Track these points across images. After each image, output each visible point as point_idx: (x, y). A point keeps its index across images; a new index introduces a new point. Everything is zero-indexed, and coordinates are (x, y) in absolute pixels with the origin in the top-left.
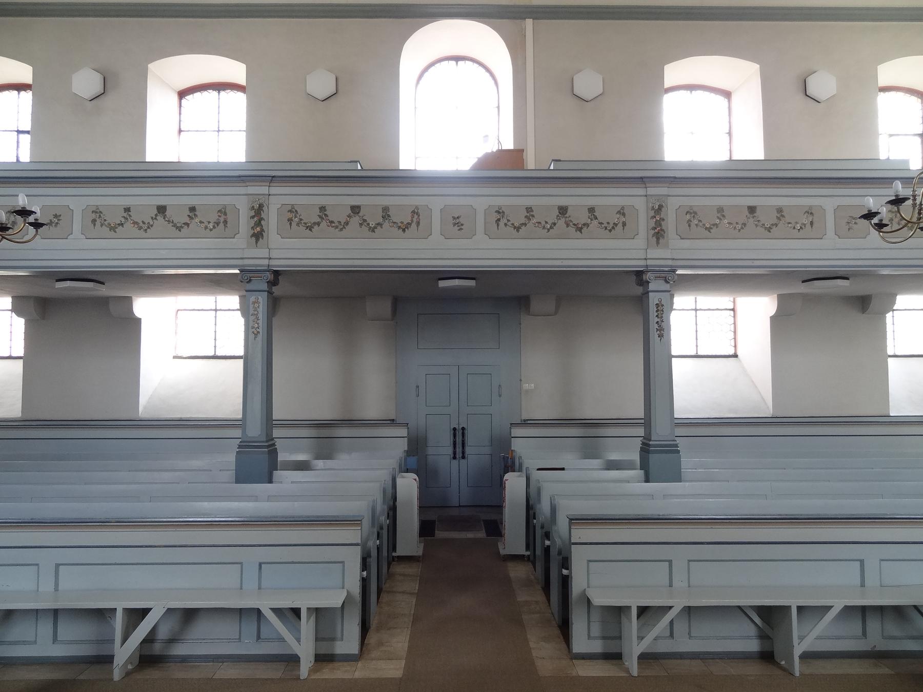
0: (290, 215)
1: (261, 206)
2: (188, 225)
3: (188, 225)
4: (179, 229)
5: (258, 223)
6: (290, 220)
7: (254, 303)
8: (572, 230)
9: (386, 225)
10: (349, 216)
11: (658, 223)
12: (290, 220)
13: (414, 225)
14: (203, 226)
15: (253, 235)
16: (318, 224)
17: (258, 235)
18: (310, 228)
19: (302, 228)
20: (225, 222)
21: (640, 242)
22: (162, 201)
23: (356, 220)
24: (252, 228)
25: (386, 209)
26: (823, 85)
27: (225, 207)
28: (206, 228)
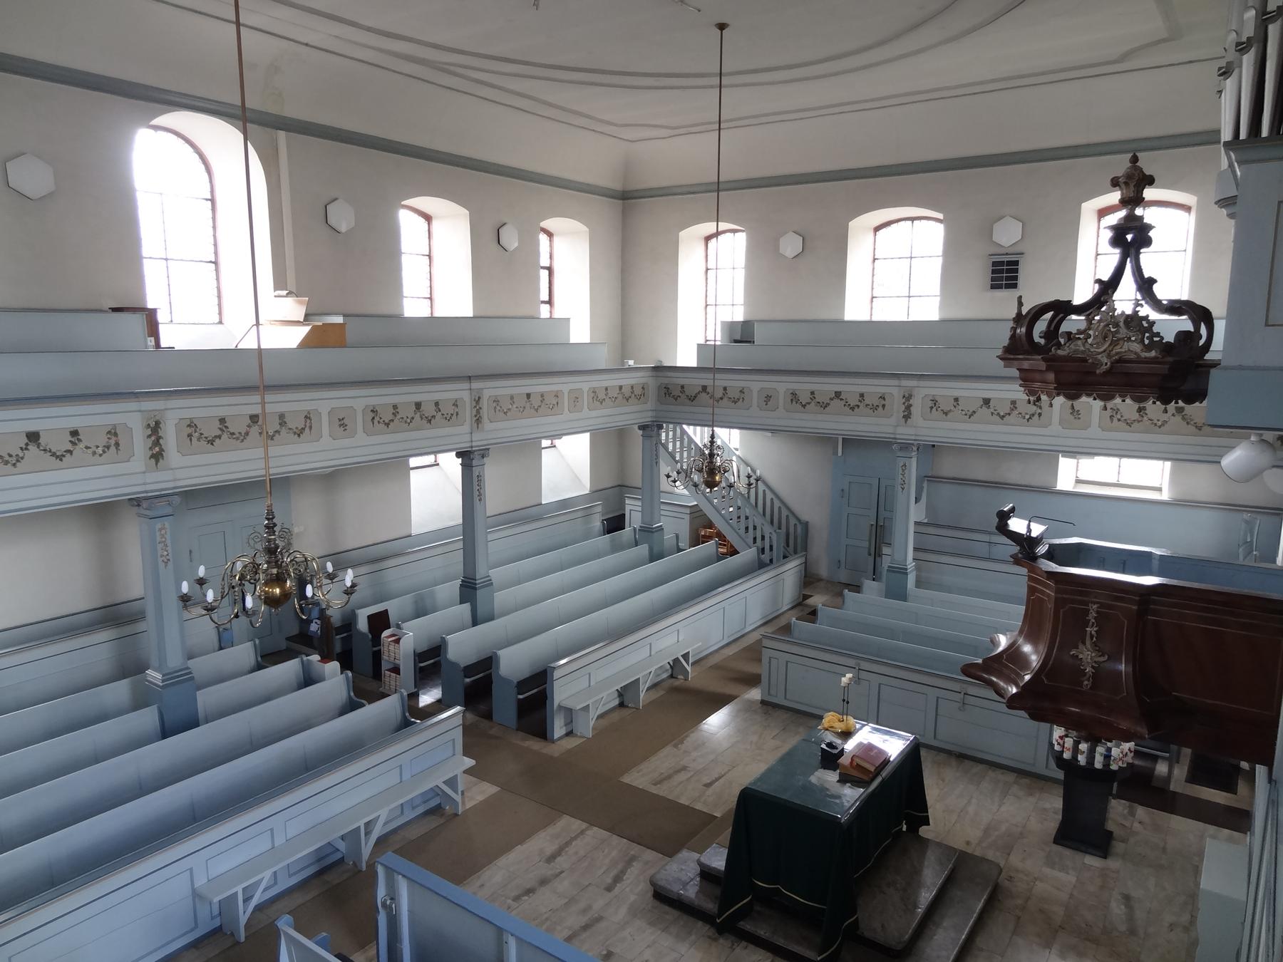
0: (189, 430)
1: (158, 423)
2: (70, 452)
3: (70, 452)
4: (60, 458)
5: (157, 443)
6: (190, 436)
7: (160, 530)
8: (425, 422)
9: (284, 431)
10: (249, 426)
11: (478, 412)
12: (190, 436)
13: (307, 429)
14: (89, 451)
15: (152, 456)
16: (220, 437)
17: (157, 456)
18: (211, 442)
19: (203, 443)
20: (117, 444)
21: (466, 428)
22: (32, 427)
23: (255, 430)
24: (151, 449)
25: (282, 416)
26: (511, 239)
27: (115, 426)
28: (94, 453)
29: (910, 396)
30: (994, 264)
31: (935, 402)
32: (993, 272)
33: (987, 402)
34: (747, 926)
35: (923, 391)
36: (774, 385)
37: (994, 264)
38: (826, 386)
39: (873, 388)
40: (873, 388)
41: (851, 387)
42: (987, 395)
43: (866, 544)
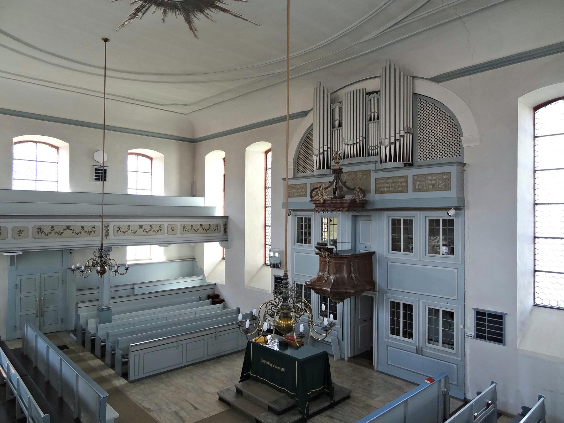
29: (108, 226)
30: (96, 170)
31: (119, 228)
32: (96, 173)
33: (141, 226)
34: (311, 412)
35: (113, 223)
36: (25, 224)
37: (96, 170)
38: (62, 223)
39: (88, 223)
40: (88, 223)
41: (76, 223)
42: (141, 224)
43: (35, 311)
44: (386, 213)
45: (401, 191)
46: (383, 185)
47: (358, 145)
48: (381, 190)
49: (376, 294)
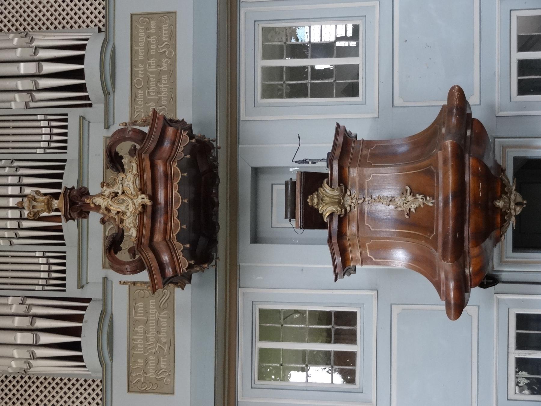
44: (246, 111)
45: (172, 35)
46: (153, 96)
47: (26, 180)
48: (164, 102)
49: (504, 148)
